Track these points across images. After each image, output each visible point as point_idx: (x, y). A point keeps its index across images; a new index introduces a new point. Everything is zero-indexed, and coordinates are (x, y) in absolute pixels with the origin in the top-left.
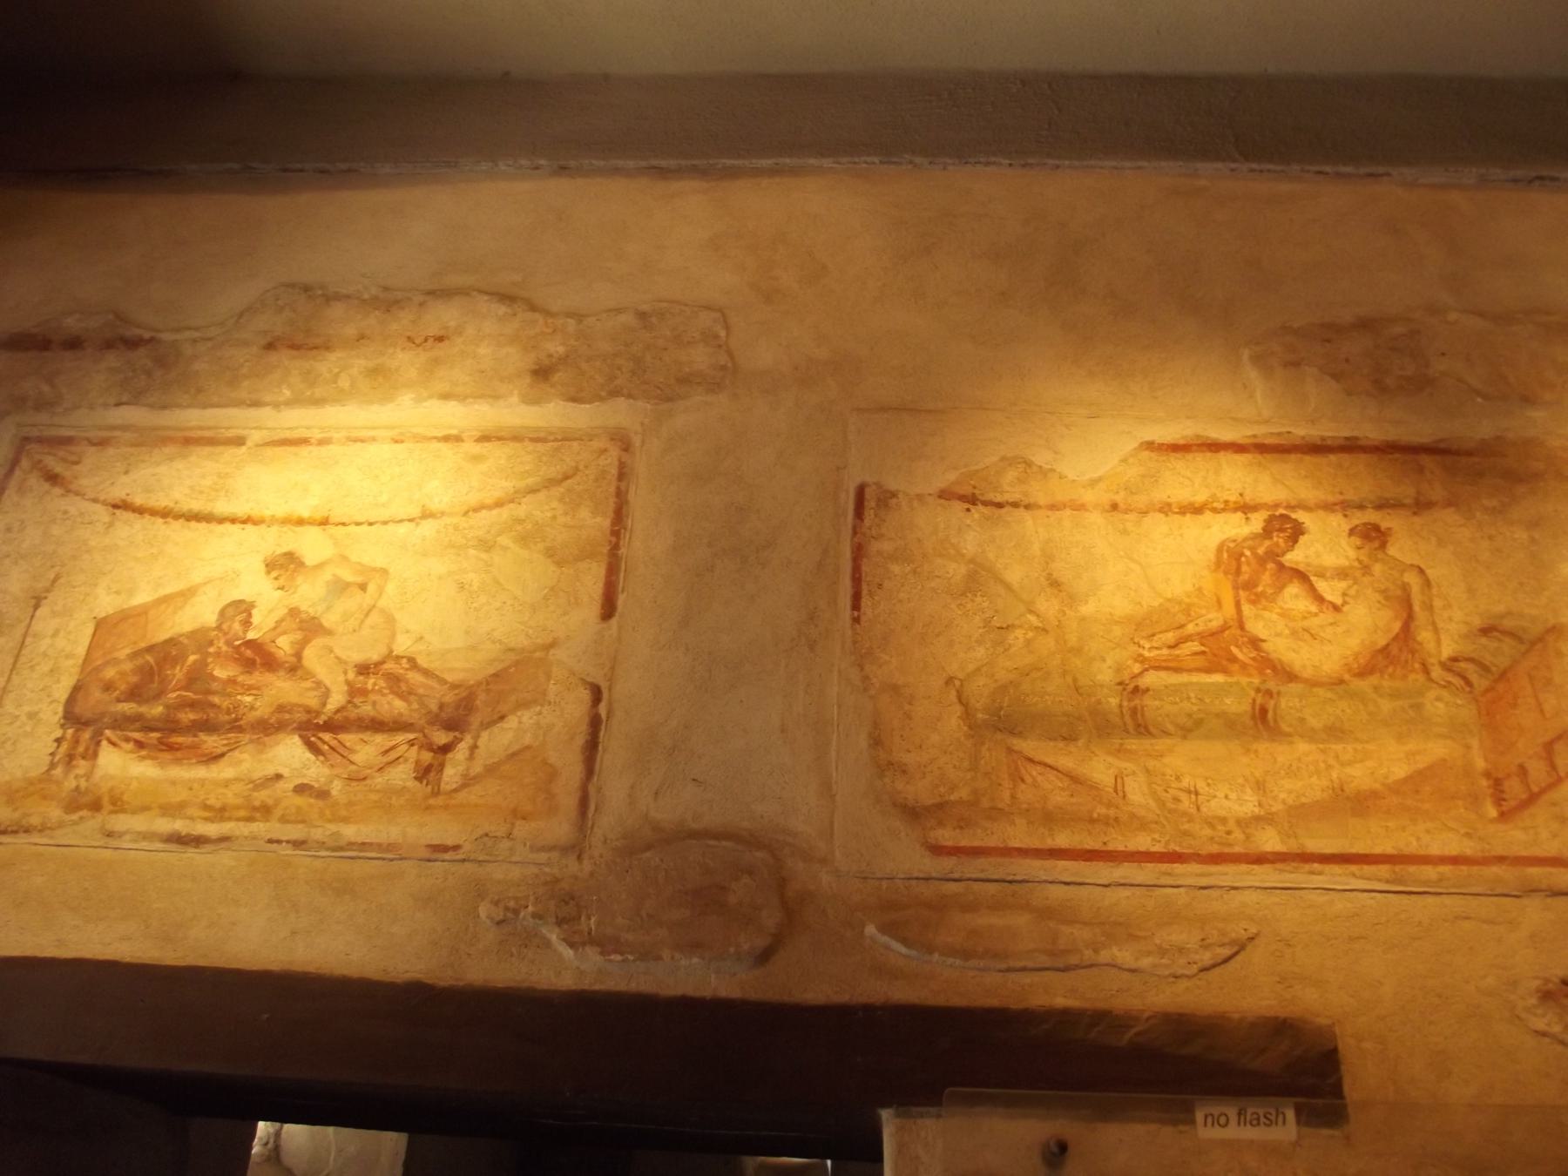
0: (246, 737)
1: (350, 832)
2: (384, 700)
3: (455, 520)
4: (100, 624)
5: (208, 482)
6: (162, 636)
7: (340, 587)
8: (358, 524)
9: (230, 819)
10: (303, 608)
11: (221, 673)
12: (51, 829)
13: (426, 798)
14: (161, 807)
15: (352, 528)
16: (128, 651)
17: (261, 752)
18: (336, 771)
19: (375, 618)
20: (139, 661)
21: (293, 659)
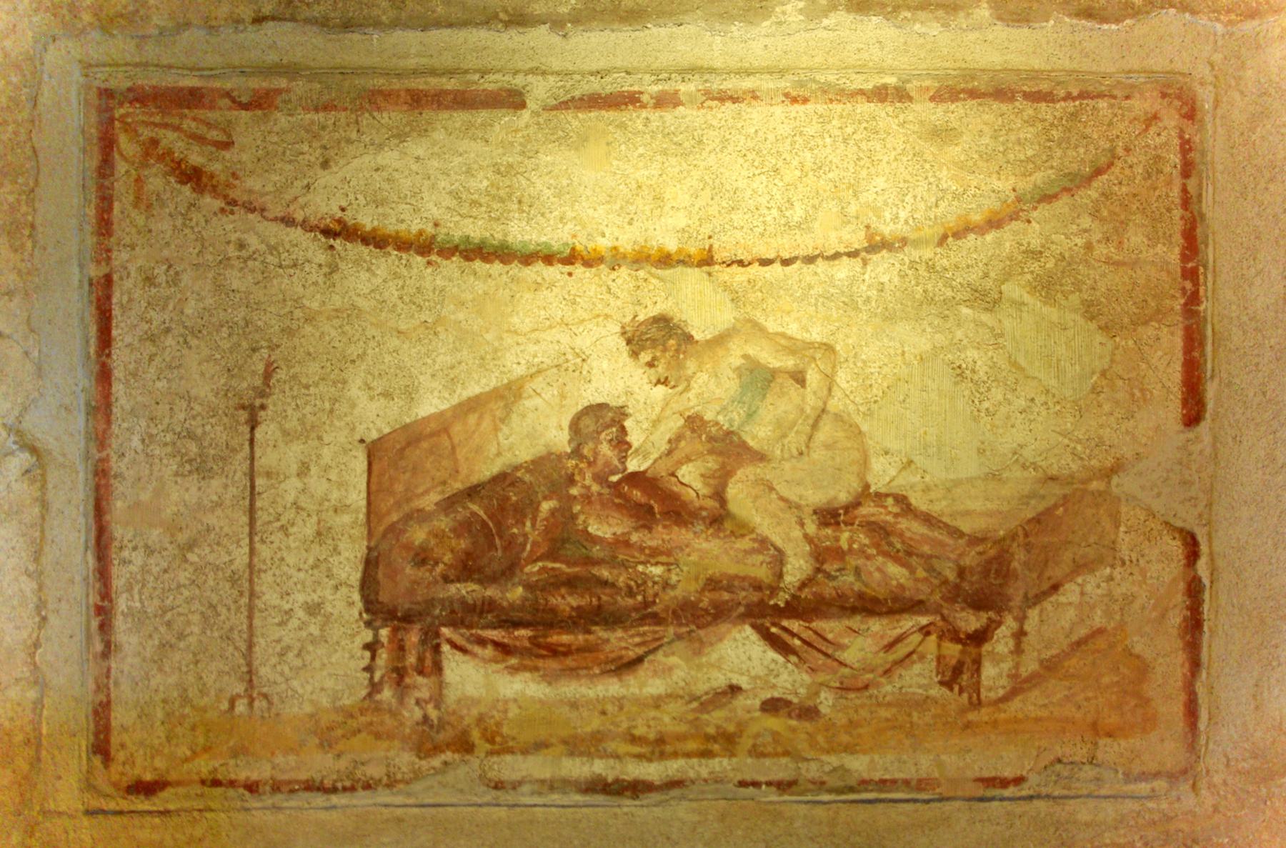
0: (671, 630)
1: (858, 765)
2: (871, 566)
3: (927, 253)
4: (373, 451)
5: (481, 183)
6: (486, 471)
7: (759, 379)
8: (765, 262)
9: (675, 755)
10: (708, 416)
11: (603, 528)
12: (407, 783)
13: (963, 711)
14: (565, 742)
15: (755, 269)
16: (434, 497)
17: (698, 653)
18: (821, 677)
19: (826, 432)
20: (461, 514)
21: (711, 503)
